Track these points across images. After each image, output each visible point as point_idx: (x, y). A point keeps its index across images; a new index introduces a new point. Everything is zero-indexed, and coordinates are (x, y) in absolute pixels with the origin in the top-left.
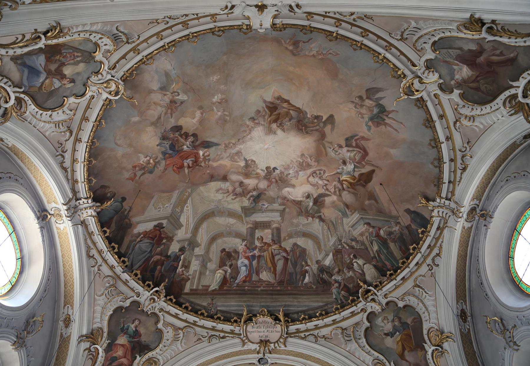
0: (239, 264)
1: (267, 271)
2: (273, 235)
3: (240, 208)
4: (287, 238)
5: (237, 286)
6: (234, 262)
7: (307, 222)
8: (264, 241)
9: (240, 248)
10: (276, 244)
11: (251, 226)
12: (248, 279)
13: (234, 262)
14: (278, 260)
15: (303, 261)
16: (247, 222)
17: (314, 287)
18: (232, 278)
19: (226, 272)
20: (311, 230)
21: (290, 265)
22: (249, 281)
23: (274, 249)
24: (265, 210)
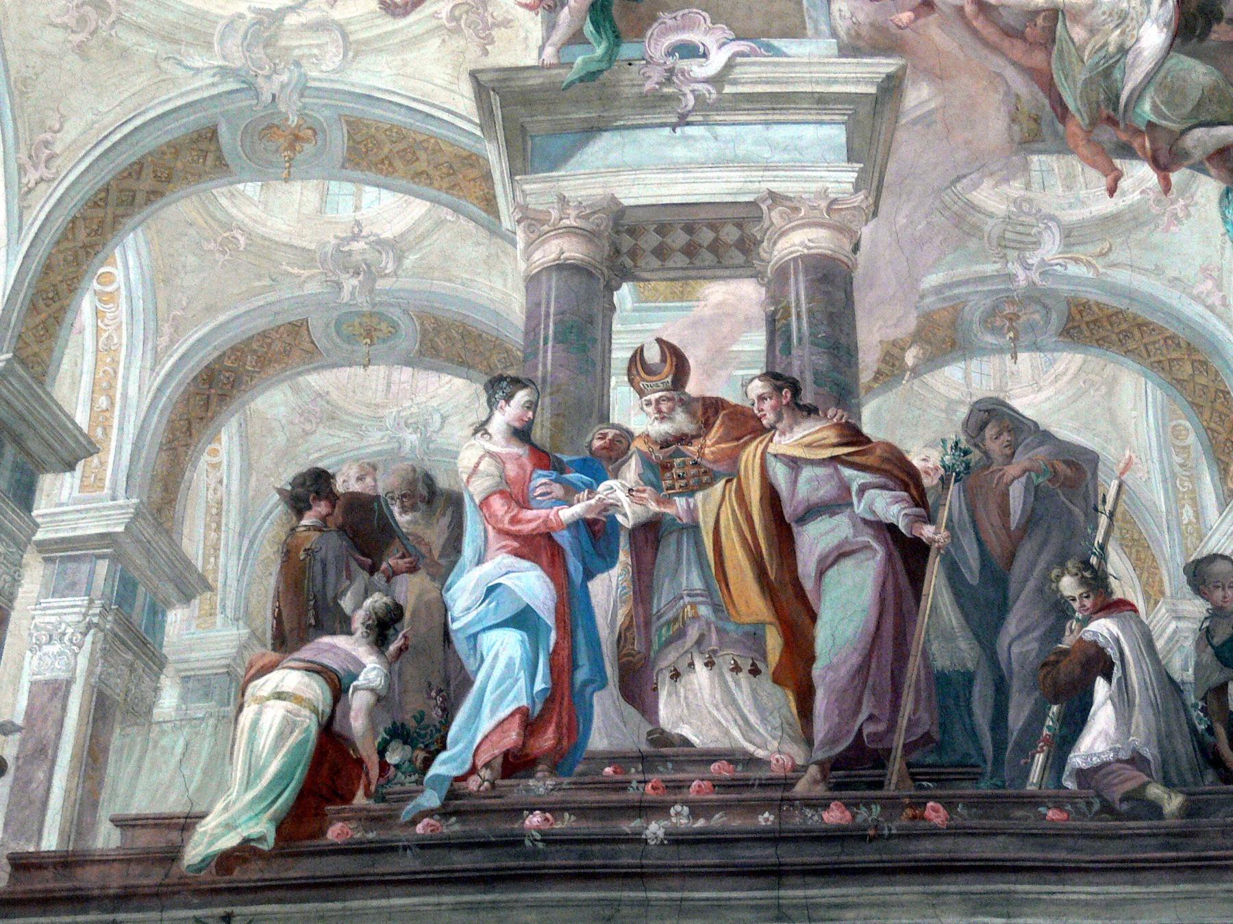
0: (457, 608)
1: (725, 661)
2: (776, 327)
3: (466, 88)
4: (910, 357)
5: (444, 812)
6: (410, 589)
7: (1106, 206)
8: (693, 388)
9: (467, 459)
10: (811, 411)
11: (572, 250)
12: (547, 739)
13: (410, 589)
14: (826, 564)
15: (1061, 561)
16: (531, 219)
17: (1173, 803)
18: (399, 733)
19: (339, 686)
20: (1146, 284)
21: (946, 601)
22: (559, 761)
23: (794, 464)
24: (702, 104)
